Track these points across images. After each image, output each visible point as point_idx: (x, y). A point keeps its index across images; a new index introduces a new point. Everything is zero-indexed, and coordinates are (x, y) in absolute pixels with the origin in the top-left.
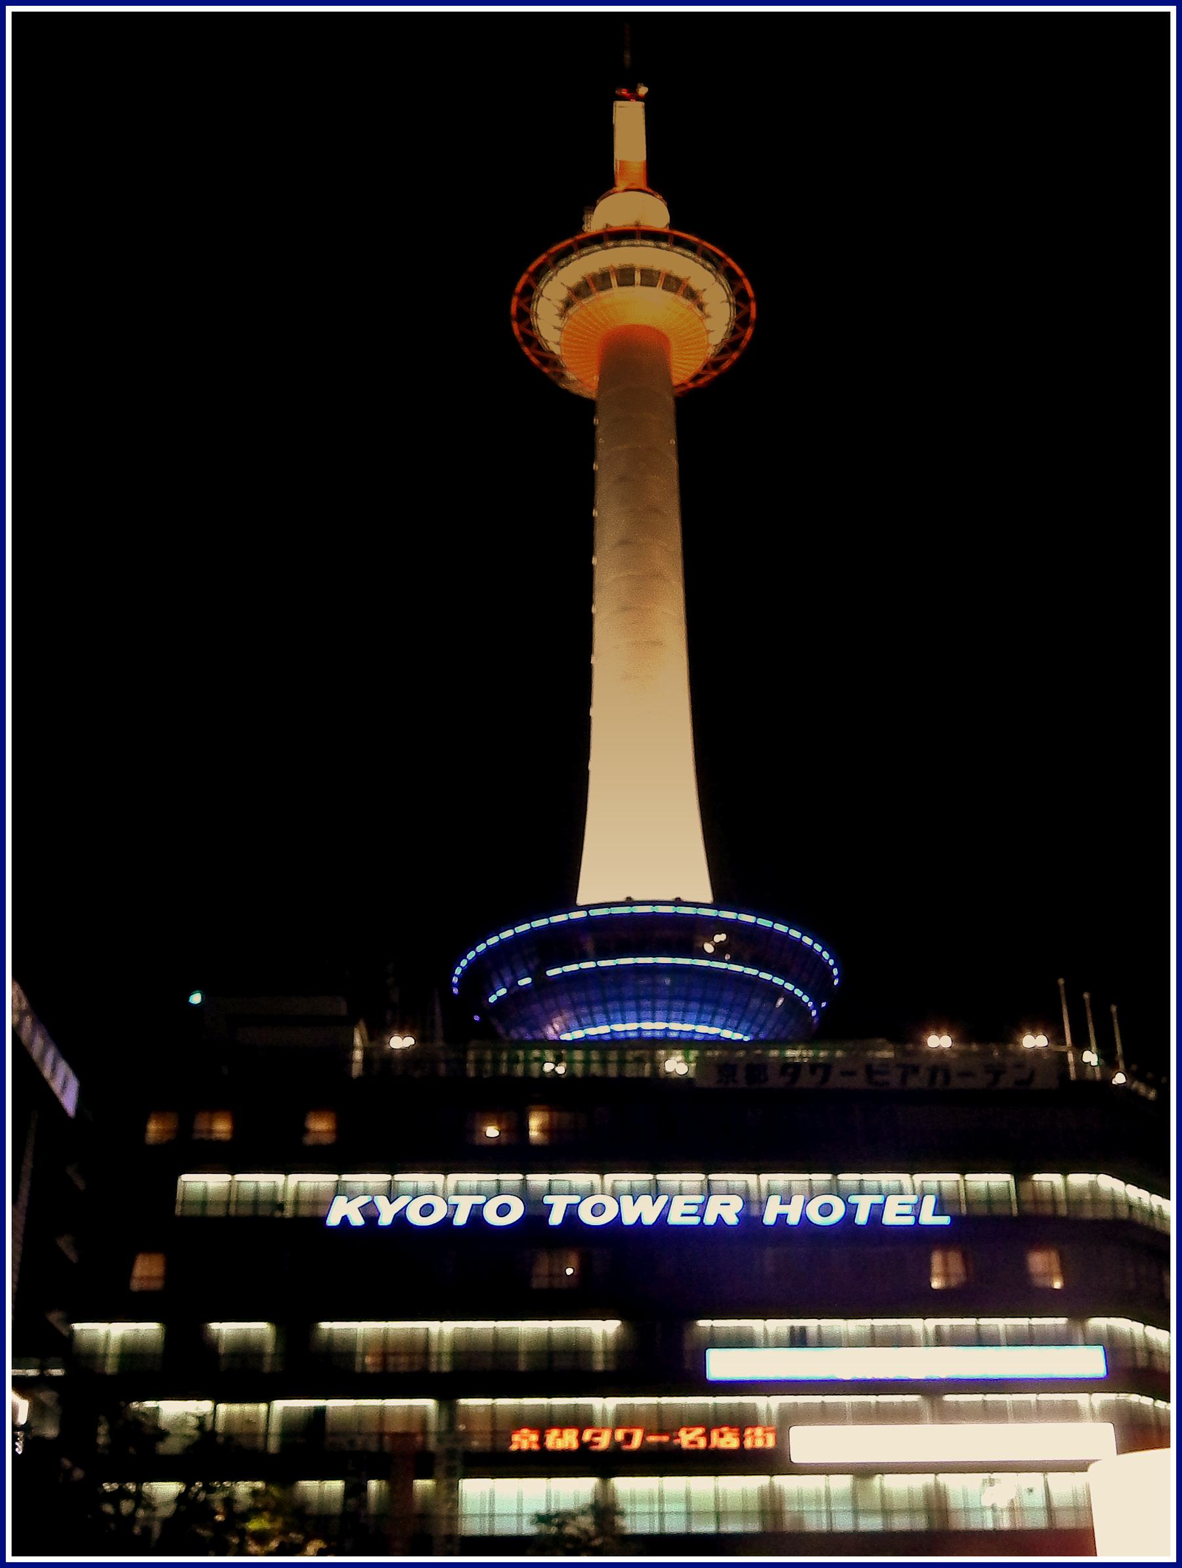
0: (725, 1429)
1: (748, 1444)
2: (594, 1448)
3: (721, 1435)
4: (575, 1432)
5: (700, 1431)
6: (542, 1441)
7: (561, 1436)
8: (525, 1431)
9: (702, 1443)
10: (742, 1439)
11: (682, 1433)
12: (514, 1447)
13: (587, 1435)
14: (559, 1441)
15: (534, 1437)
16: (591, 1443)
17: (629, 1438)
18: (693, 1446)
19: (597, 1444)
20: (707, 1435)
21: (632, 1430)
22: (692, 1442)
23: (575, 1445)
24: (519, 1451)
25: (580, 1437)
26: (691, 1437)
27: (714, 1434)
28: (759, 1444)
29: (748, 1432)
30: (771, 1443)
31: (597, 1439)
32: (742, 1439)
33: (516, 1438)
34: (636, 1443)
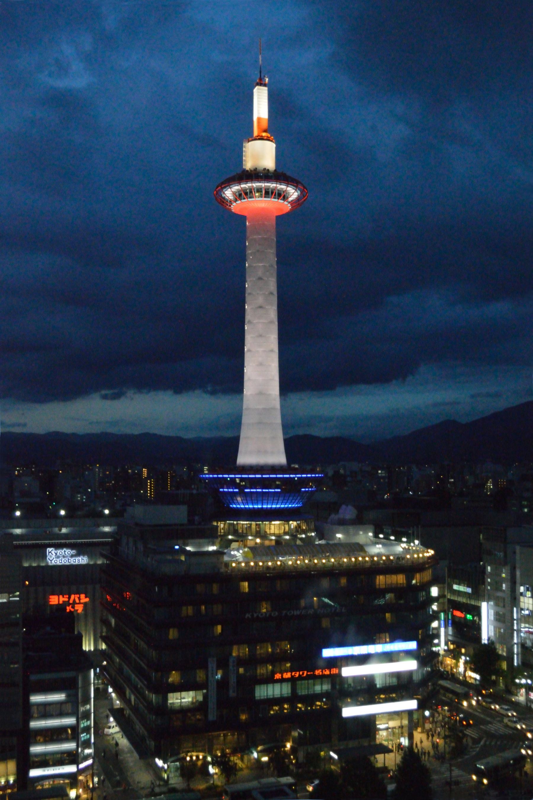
0: (326, 670)
1: (332, 673)
2: (295, 677)
3: (325, 671)
4: (290, 673)
5: (320, 670)
6: (282, 676)
7: (287, 674)
8: (278, 674)
9: (321, 674)
10: (330, 671)
11: (316, 671)
12: (275, 678)
13: (293, 674)
14: (286, 676)
15: (280, 675)
16: (294, 675)
17: (303, 674)
18: (318, 674)
19: (295, 676)
20: (322, 672)
21: (304, 672)
22: (318, 673)
23: (290, 677)
24: (277, 679)
25: (291, 674)
26: (318, 672)
27: (324, 671)
28: (334, 672)
29: (332, 669)
30: (337, 672)
31: (295, 675)
32: (330, 671)
33: (276, 676)
34: (305, 675)
